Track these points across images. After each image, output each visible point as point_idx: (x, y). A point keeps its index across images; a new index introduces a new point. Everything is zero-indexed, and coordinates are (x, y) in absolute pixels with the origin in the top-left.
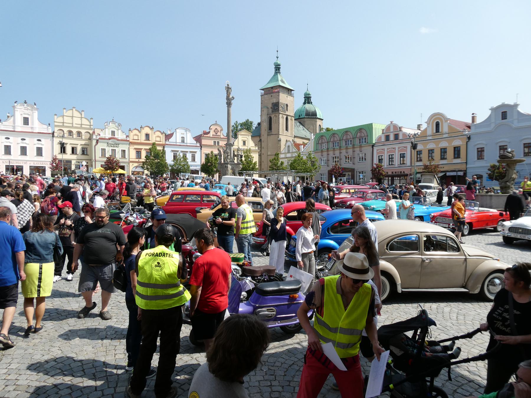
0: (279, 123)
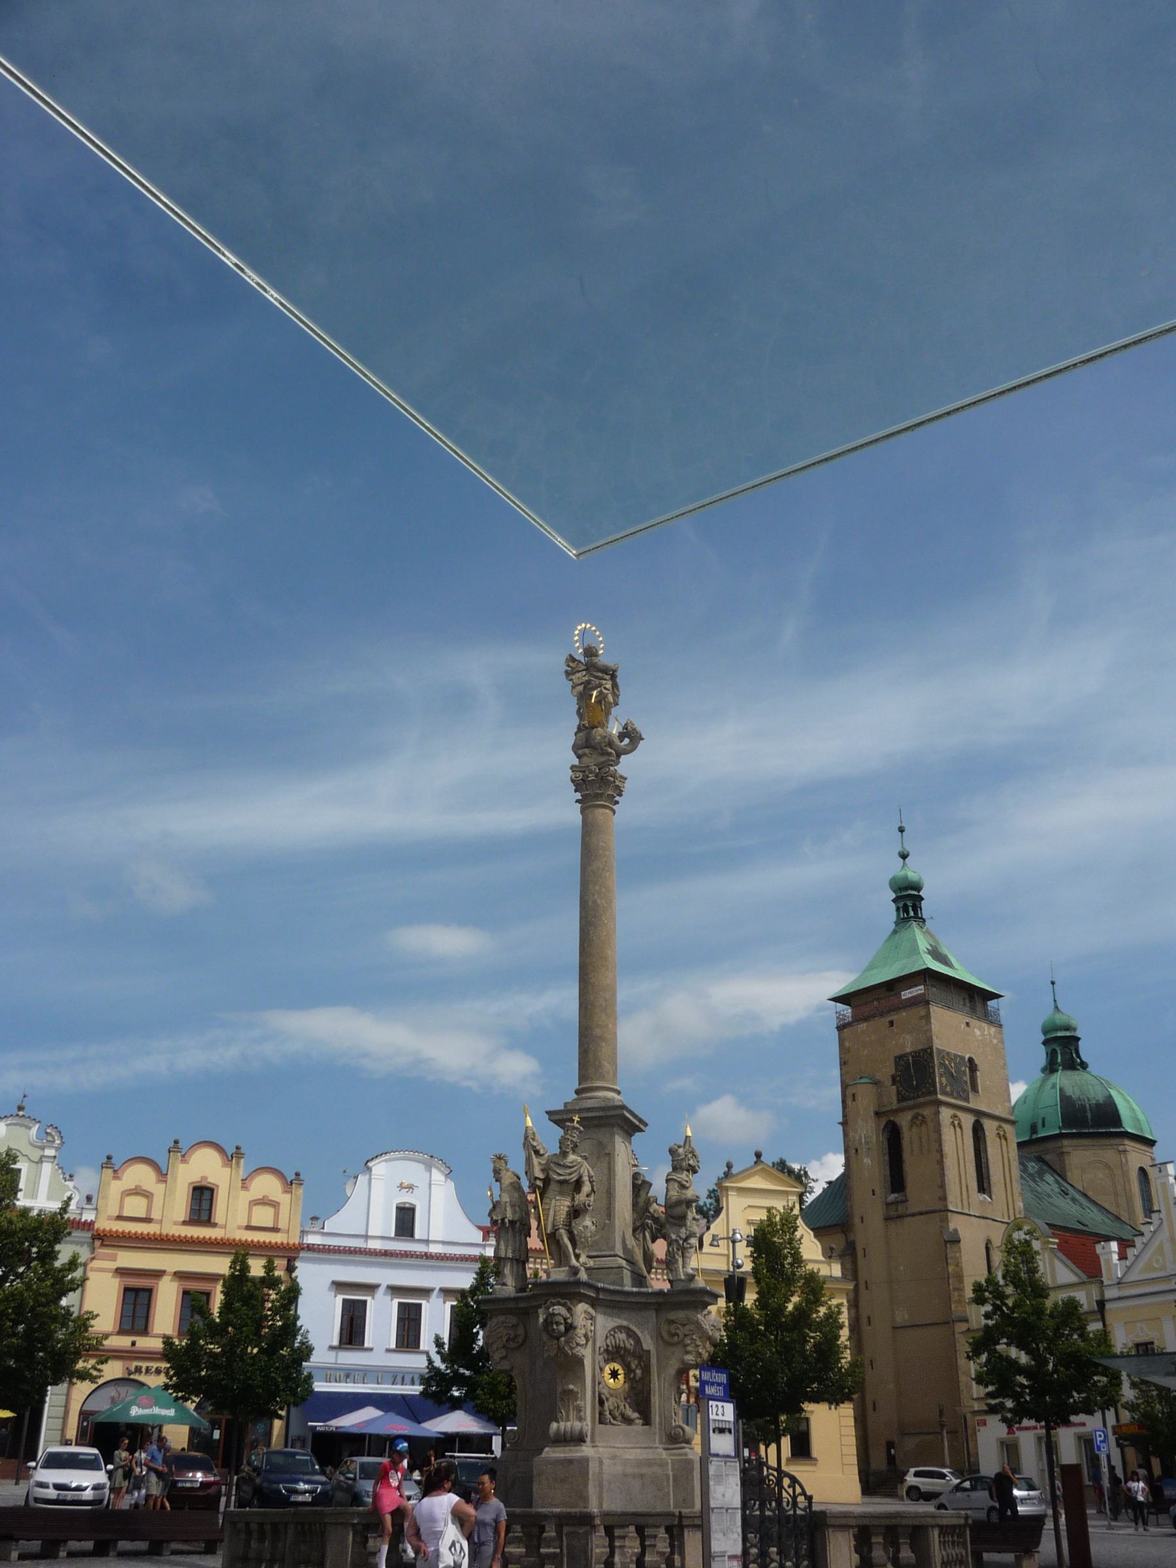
0: (940, 1150)
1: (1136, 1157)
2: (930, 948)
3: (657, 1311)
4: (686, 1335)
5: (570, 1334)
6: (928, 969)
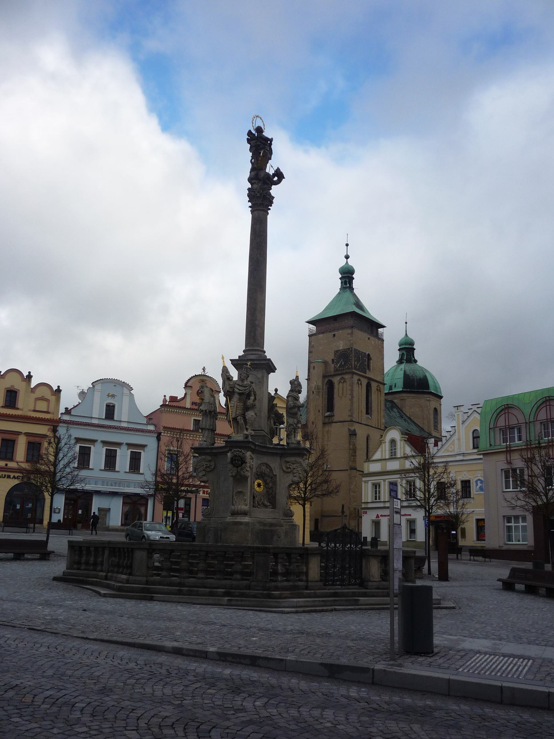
0: (352, 395)
1: (433, 404)
2: (355, 302)
3: (281, 457)
4: (294, 469)
5: (243, 465)
6: (354, 312)
